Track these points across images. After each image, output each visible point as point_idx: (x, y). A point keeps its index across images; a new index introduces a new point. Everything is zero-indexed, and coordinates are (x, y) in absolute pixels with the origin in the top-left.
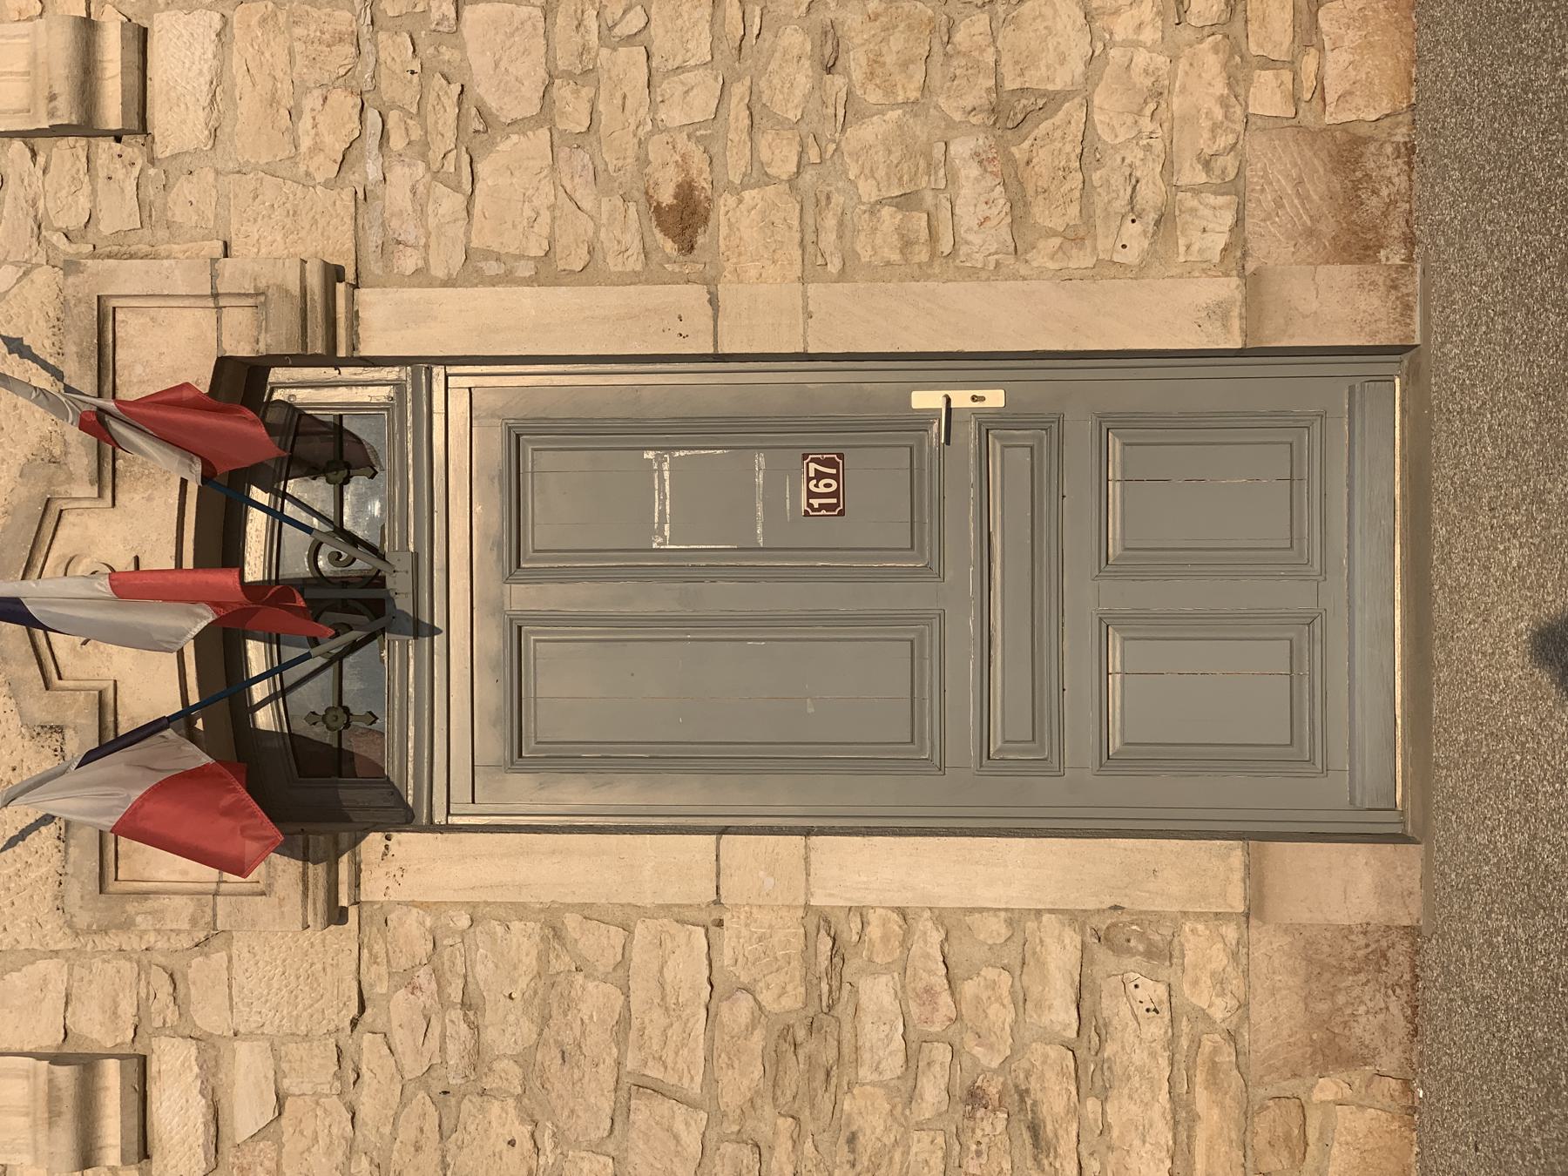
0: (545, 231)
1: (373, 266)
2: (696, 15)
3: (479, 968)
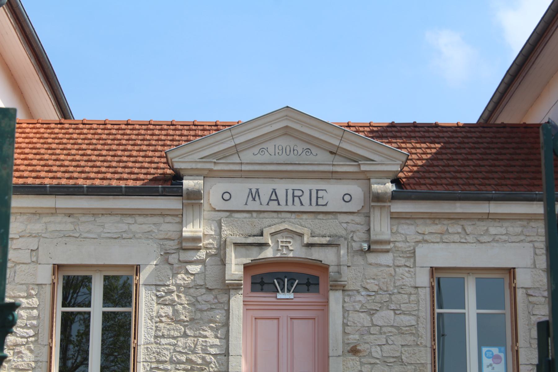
0: (352, 325)
1: (346, 293)
2: (391, 353)
3: (218, 311)
